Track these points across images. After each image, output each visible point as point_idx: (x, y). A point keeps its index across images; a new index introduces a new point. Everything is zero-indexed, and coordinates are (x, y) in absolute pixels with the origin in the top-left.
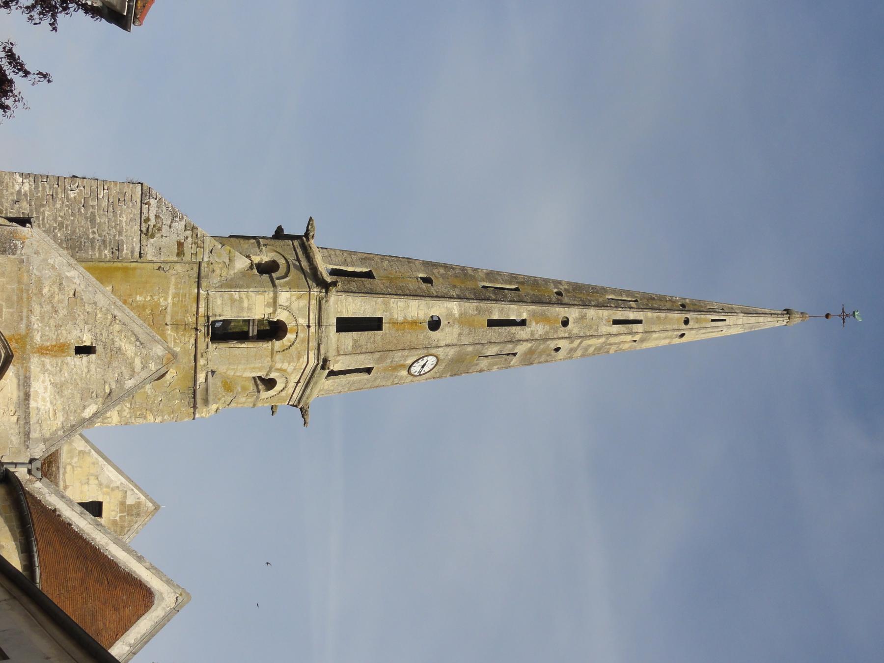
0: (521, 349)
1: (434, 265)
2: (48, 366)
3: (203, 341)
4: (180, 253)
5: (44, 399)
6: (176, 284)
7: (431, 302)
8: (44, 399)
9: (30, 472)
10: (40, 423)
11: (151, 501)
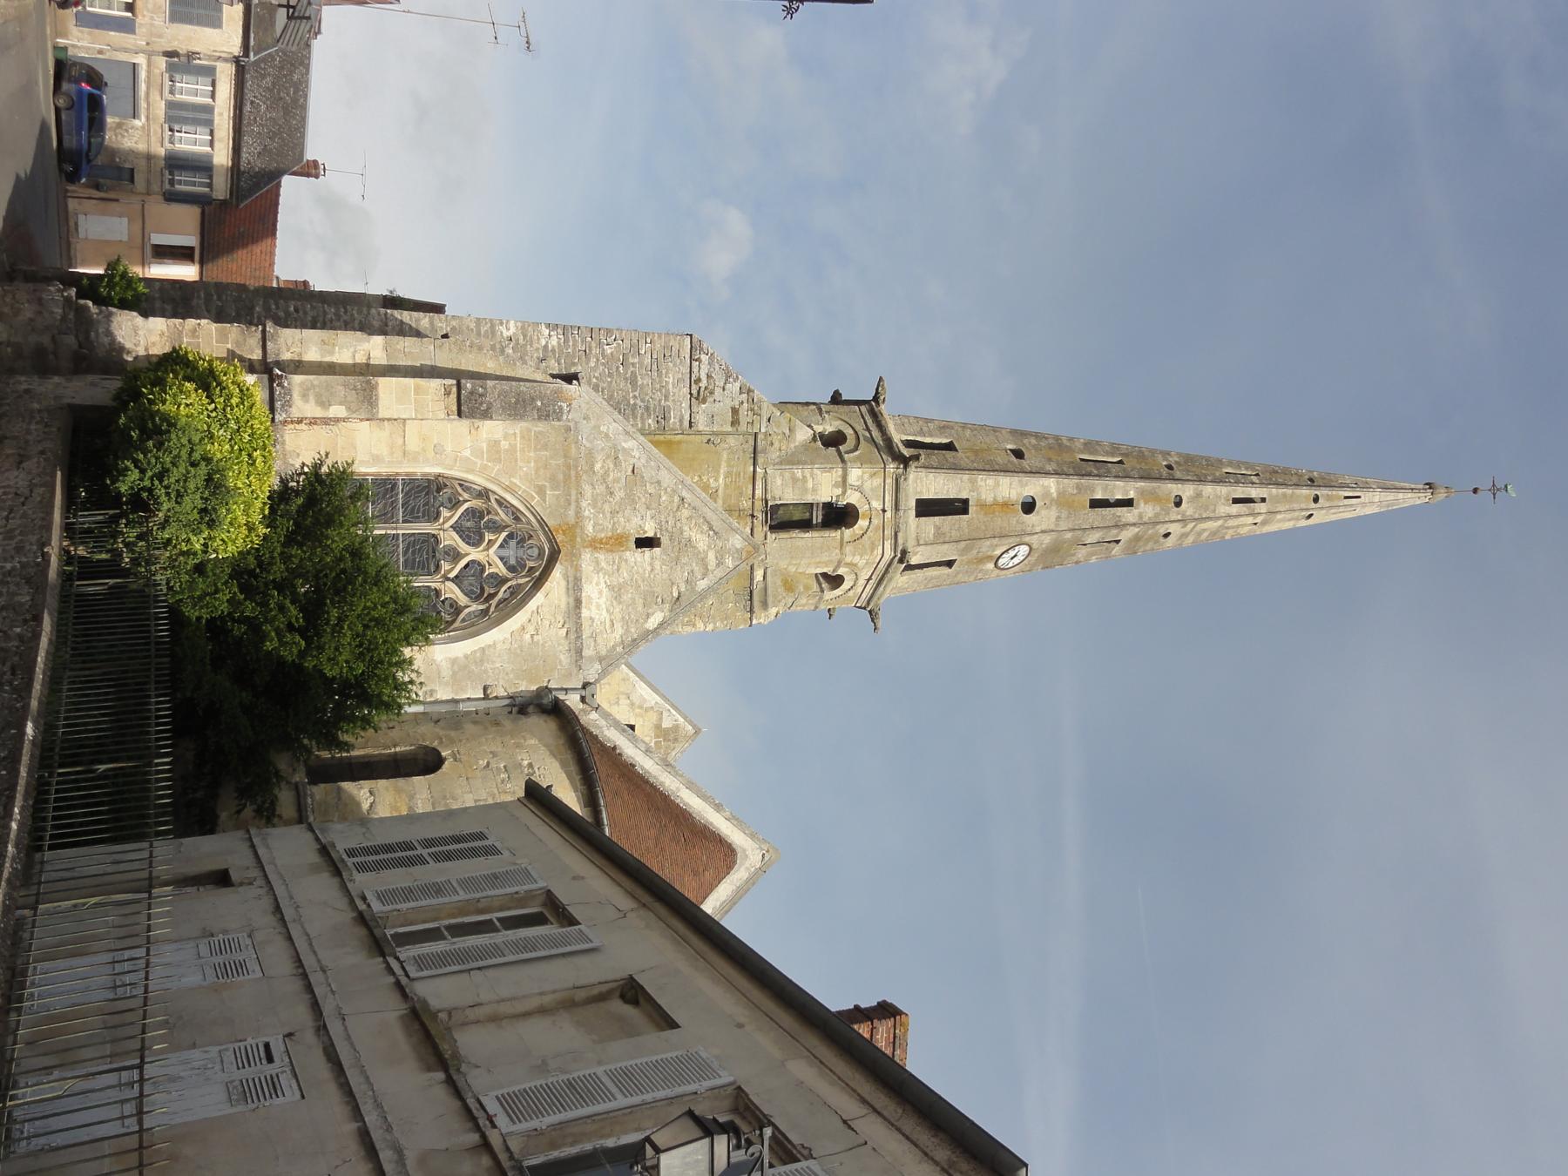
0: (1126, 535)
1: (1024, 434)
2: (603, 564)
3: (761, 530)
4: (735, 423)
5: (598, 606)
7: (1025, 479)
8: (598, 606)
9: (583, 699)
10: (594, 637)
11: (691, 723)
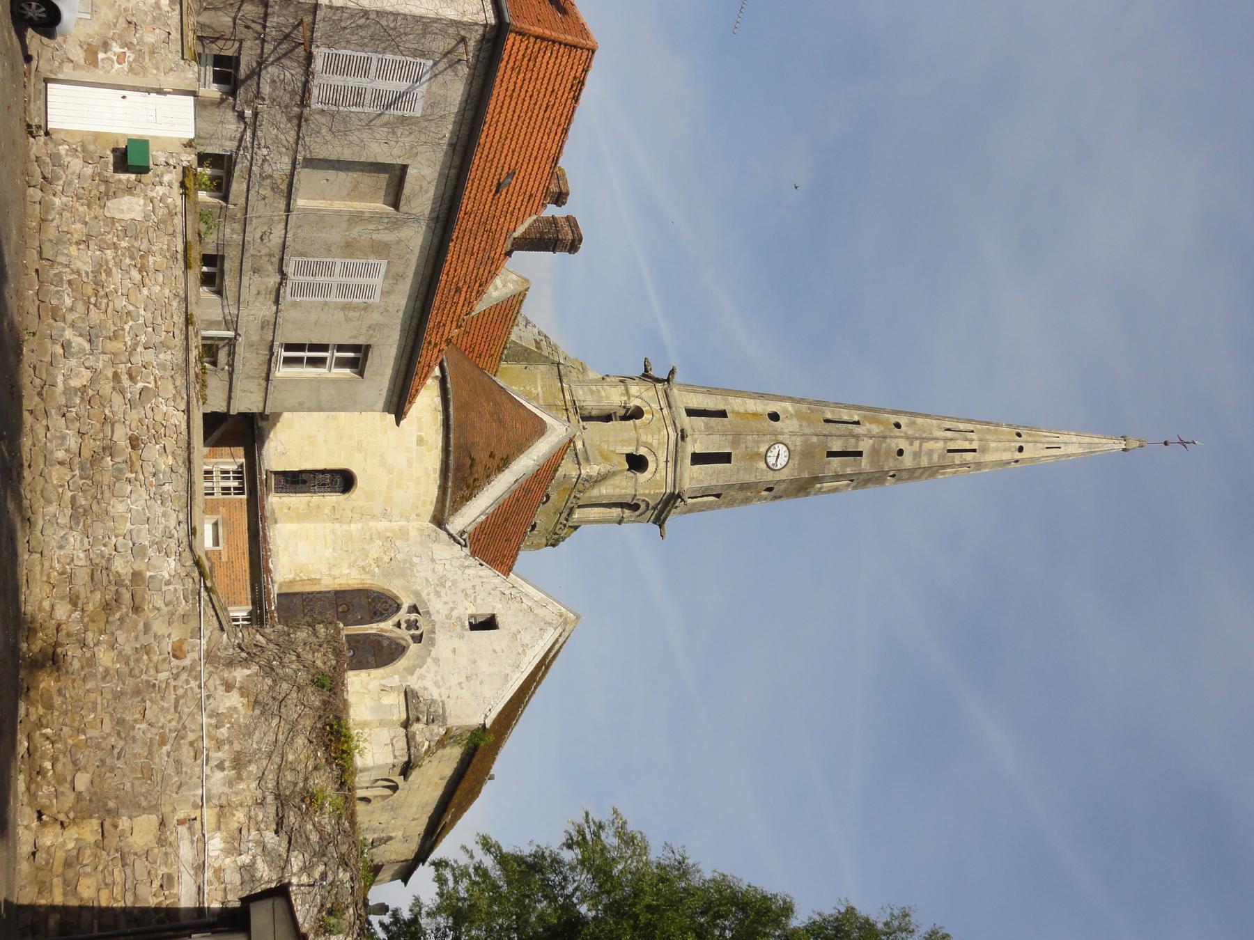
6: (542, 379)
